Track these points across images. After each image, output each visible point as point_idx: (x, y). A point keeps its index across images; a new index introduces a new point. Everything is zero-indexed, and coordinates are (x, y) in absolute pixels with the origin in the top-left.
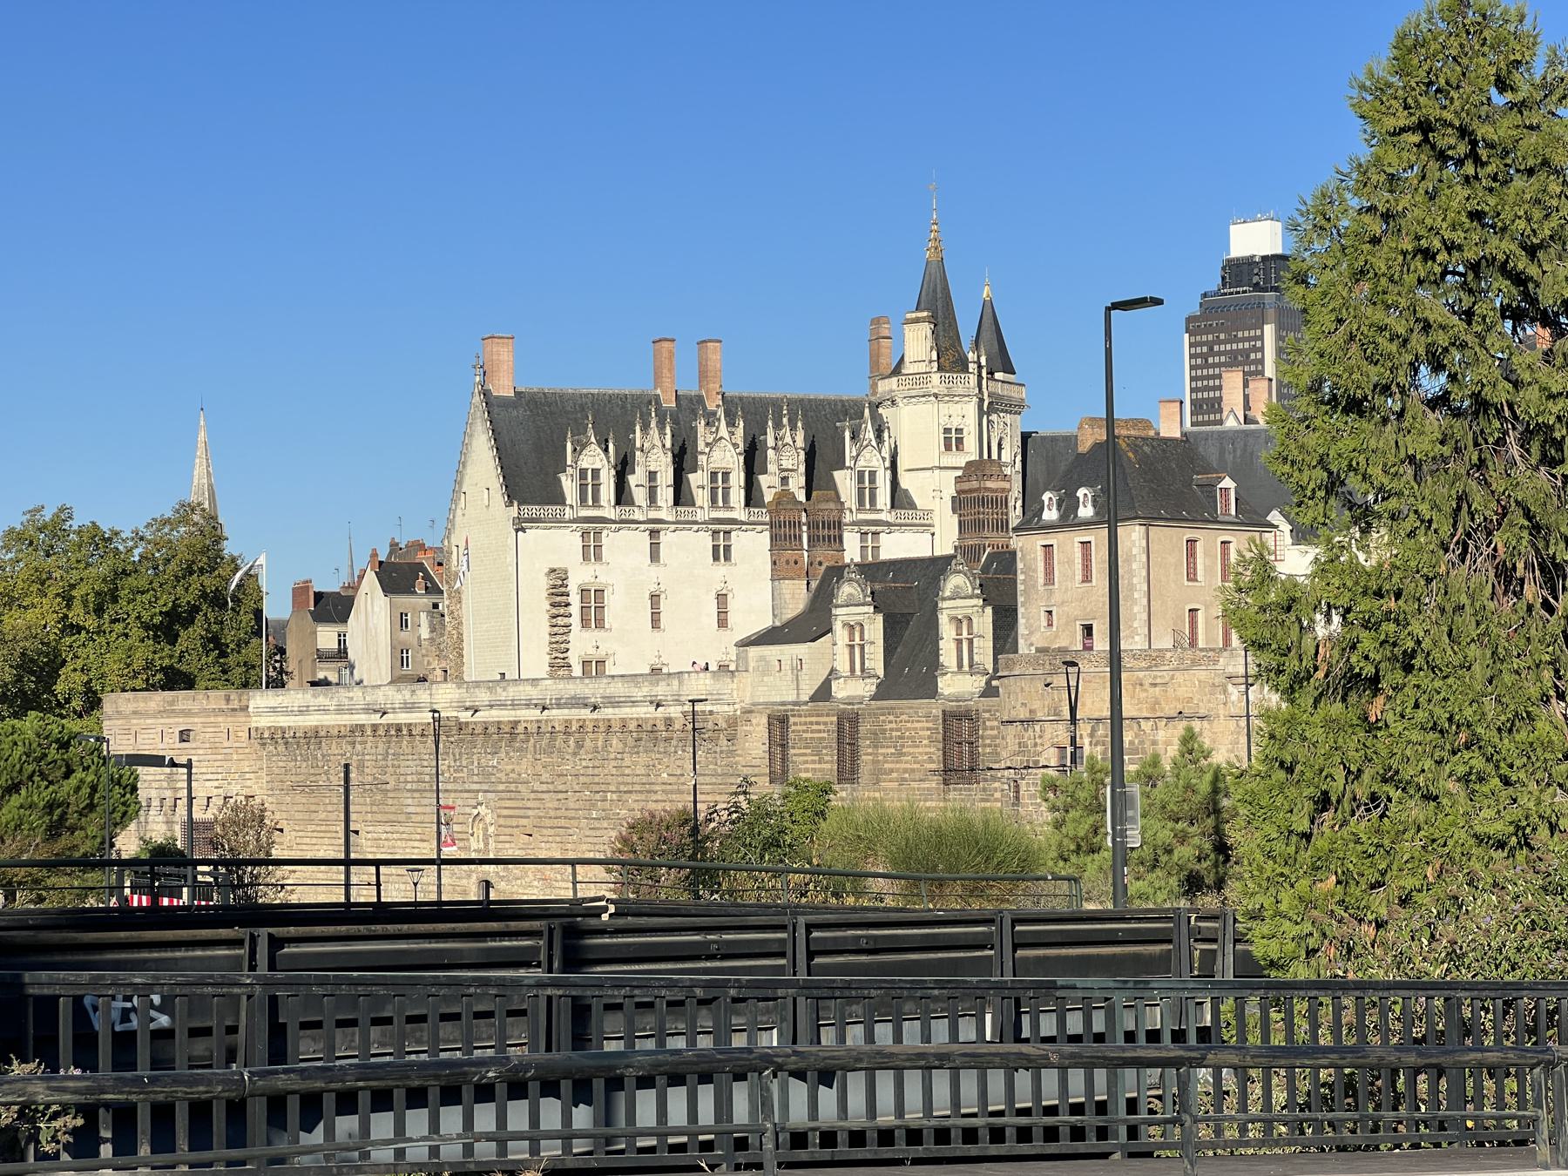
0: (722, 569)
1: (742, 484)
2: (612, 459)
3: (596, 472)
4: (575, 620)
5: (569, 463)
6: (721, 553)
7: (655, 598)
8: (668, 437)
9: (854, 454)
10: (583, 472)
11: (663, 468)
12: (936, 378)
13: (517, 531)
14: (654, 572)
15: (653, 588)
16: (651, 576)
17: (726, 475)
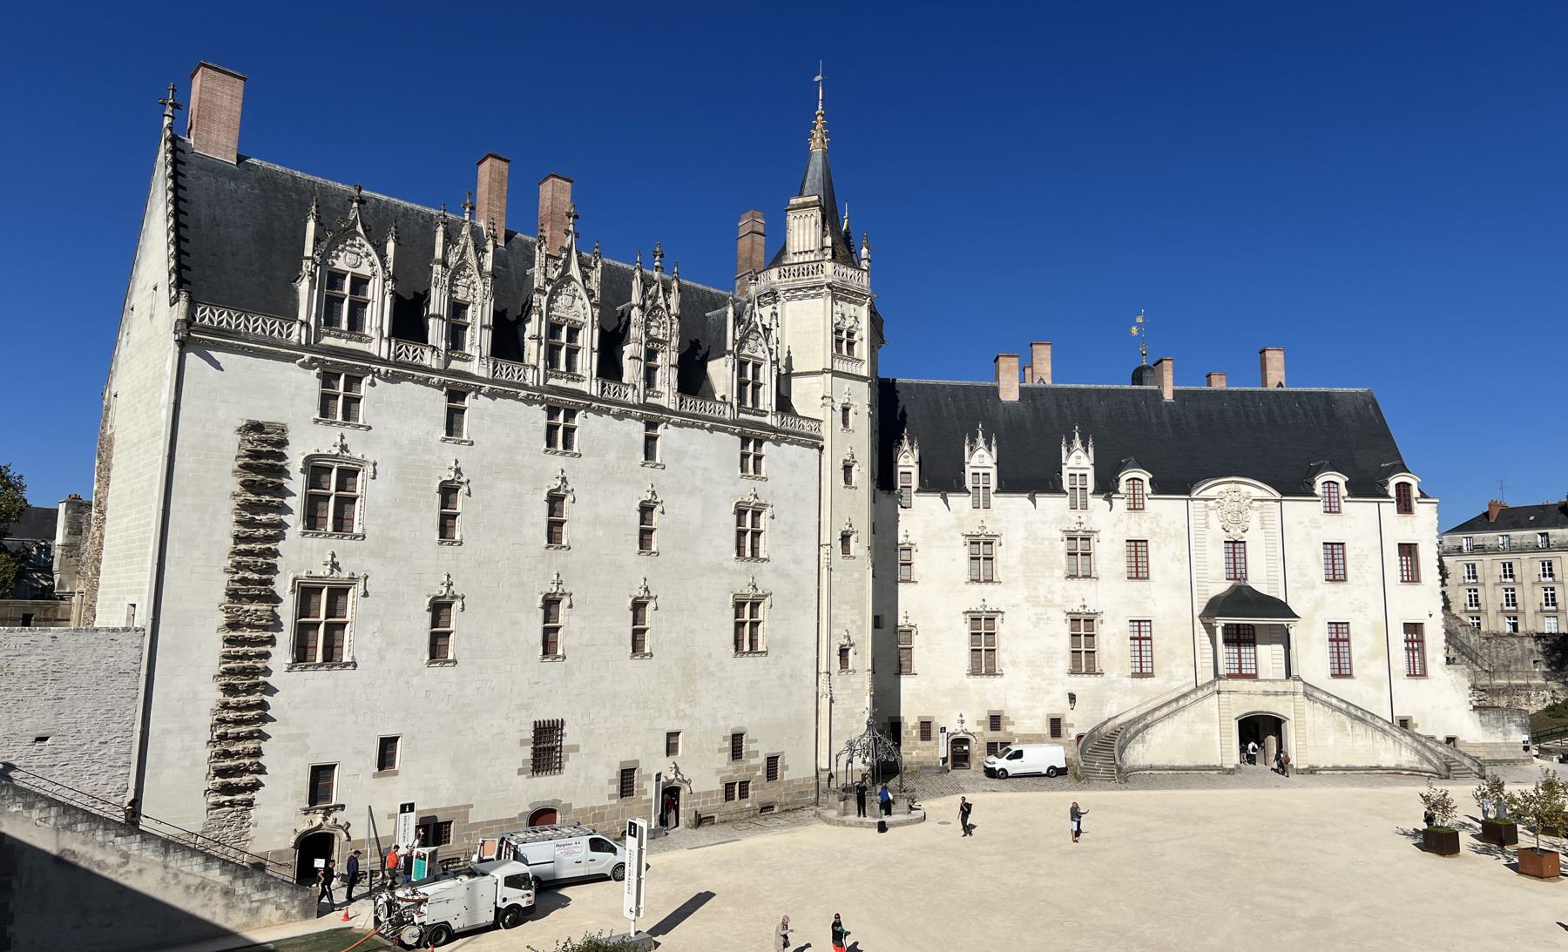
0: (557, 462)
1: (596, 346)
2: (391, 266)
3: (360, 283)
4: (295, 521)
5: (308, 252)
6: (558, 437)
7: (448, 492)
8: (490, 255)
9: (737, 338)
10: (335, 278)
11: (478, 300)
12: (829, 267)
13: (184, 345)
14: (451, 453)
15: (449, 475)
16: (444, 459)
17: (573, 332)
